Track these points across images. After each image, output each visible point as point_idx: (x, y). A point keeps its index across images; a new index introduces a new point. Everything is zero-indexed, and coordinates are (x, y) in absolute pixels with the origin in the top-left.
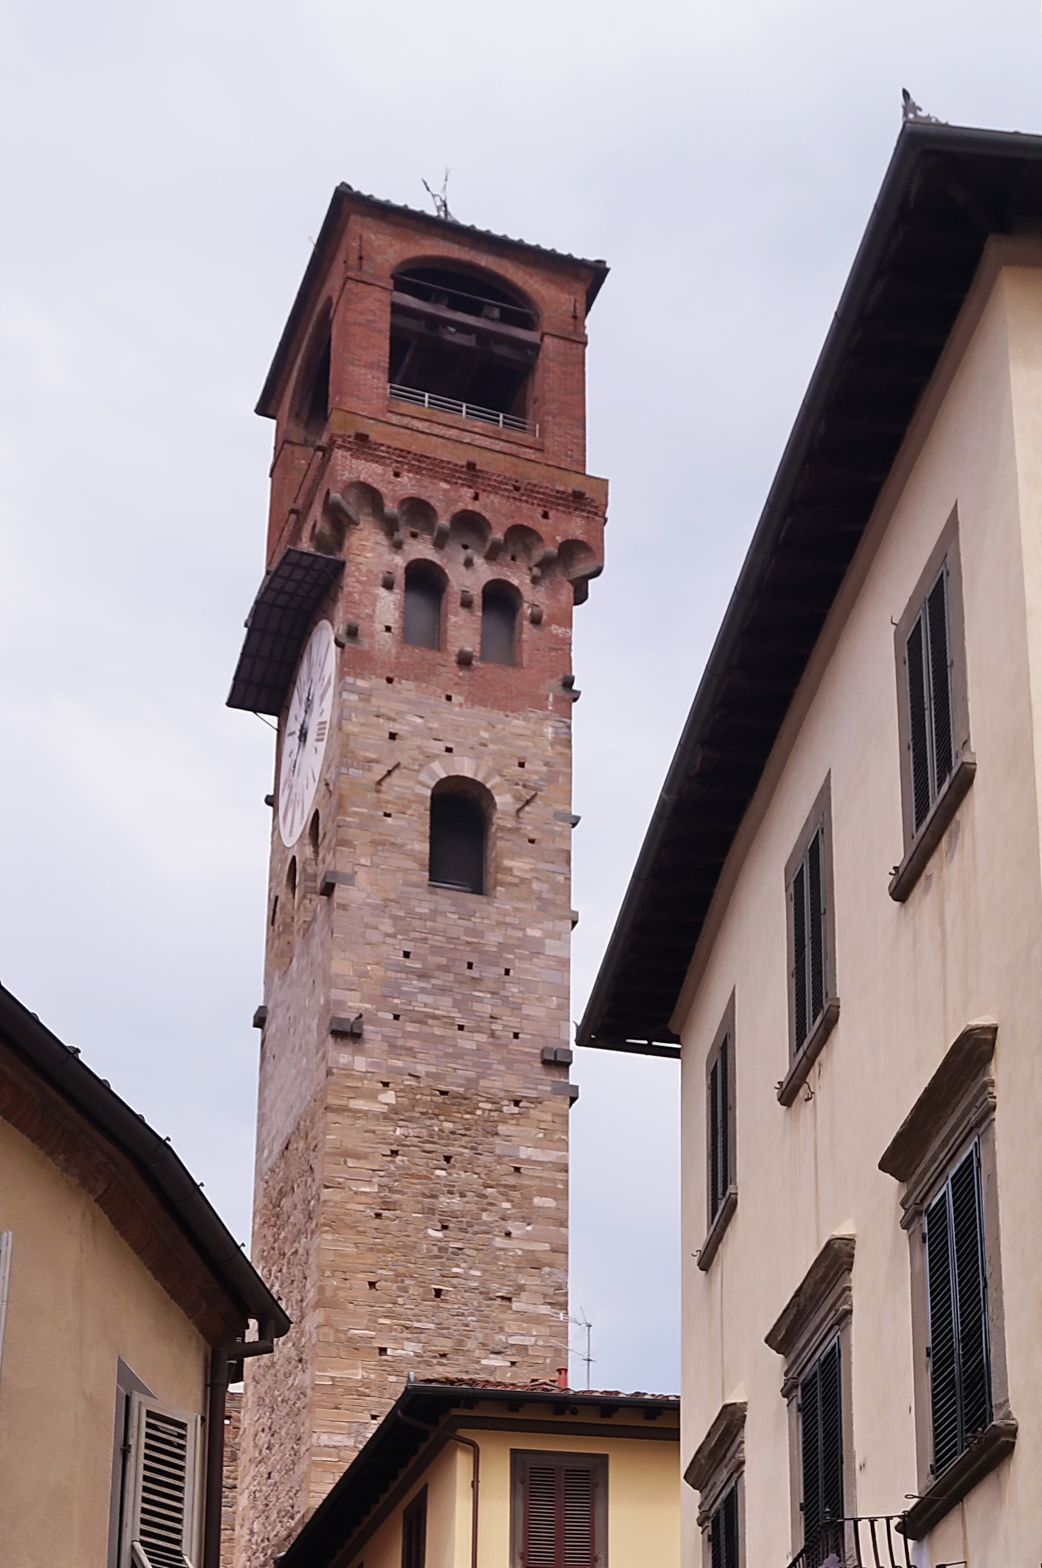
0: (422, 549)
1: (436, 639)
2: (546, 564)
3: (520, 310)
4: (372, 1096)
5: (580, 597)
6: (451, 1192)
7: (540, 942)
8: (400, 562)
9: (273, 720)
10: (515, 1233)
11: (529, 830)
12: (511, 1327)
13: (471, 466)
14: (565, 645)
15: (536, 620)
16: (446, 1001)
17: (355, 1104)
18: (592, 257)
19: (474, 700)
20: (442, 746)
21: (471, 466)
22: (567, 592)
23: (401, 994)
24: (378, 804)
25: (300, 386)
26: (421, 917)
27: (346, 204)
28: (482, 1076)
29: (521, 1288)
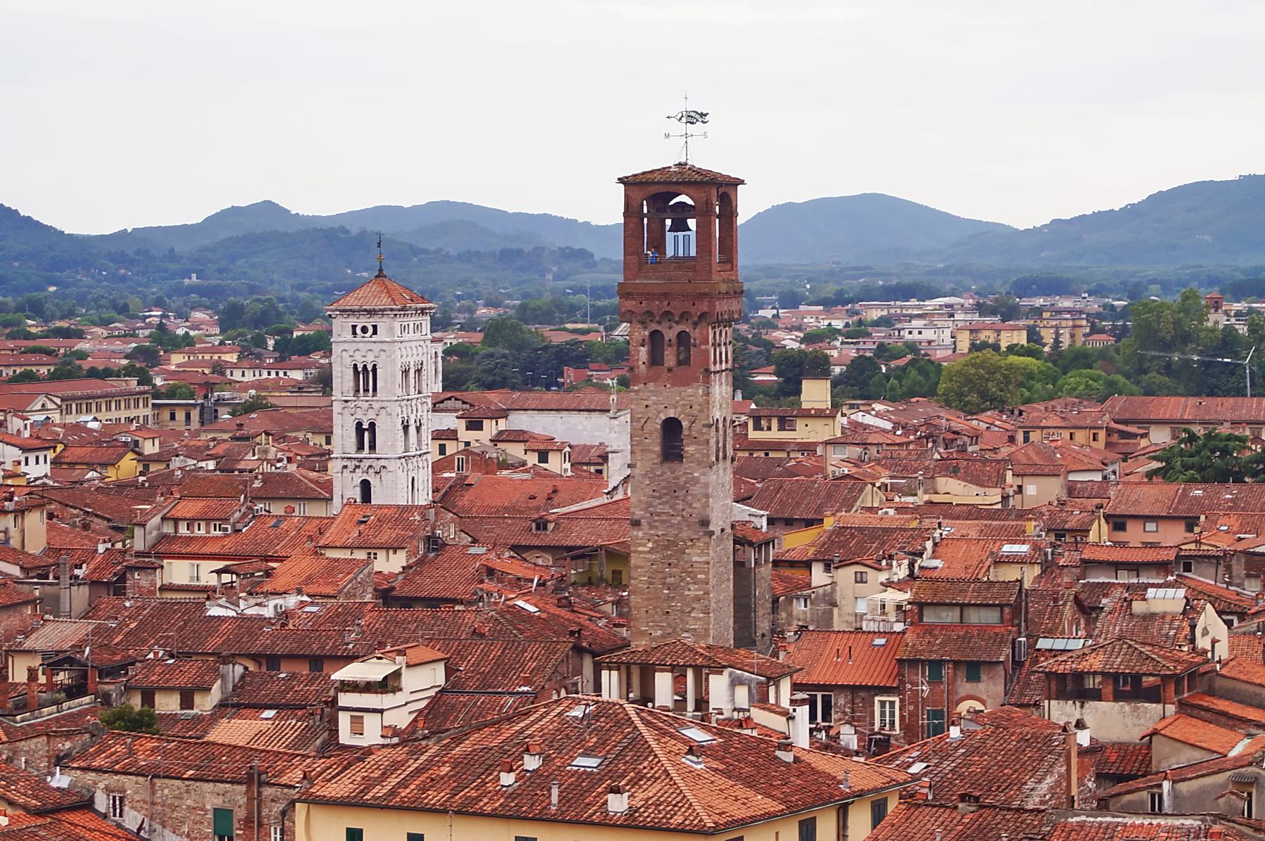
0: (654, 327)
4: (645, 545)
8: (647, 333)
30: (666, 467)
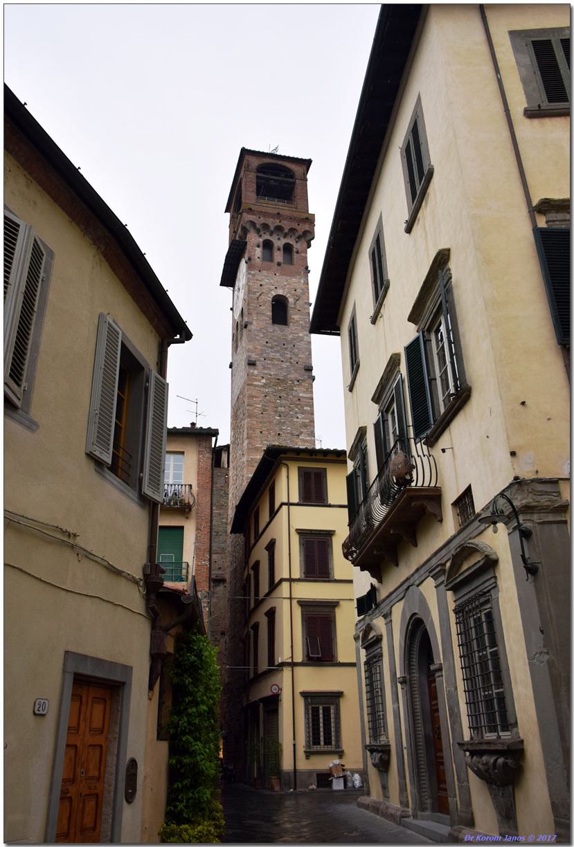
0: (267, 237)
1: (271, 259)
2: (299, 237)
3: (290, 174)
4: (259, 381)
5: (309, 246)
6: (281, 406)
7: (303, 337)
8: (261, 240)
9: (232, 288)
10: (299, 417)
11: (298, 307)
12: (300, 443)
13: (278, 214)
14: (306, 258)
15: (297, 252)
16: (278, 354)
17: (255, 383)
18: (307, 158)
19: (282, 274)
20: (274, 287)
21: (278, 214)
22: (305, 245)
23: (266, 353)
24: (258, 303)
25: (235, 204)
26: (270, 332)
27: (244, 152)
28: (288, 374)
29: (302, 432)
30: (277, 327)
